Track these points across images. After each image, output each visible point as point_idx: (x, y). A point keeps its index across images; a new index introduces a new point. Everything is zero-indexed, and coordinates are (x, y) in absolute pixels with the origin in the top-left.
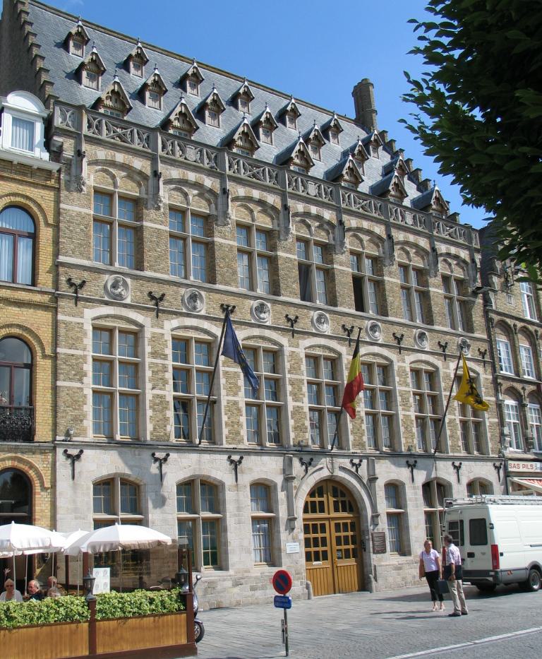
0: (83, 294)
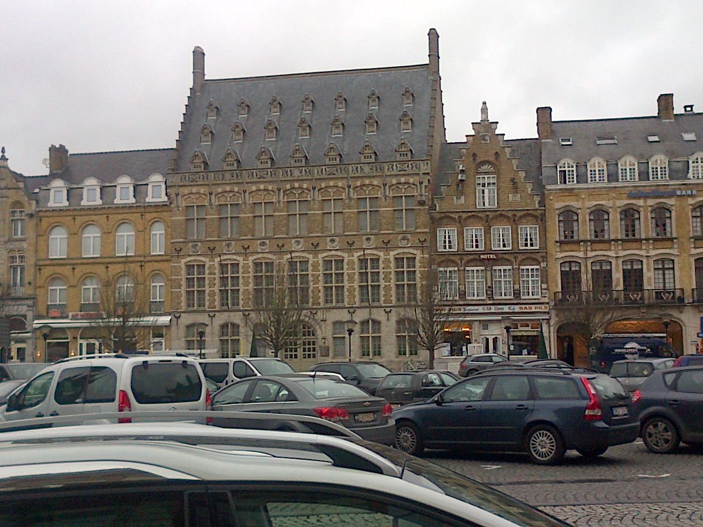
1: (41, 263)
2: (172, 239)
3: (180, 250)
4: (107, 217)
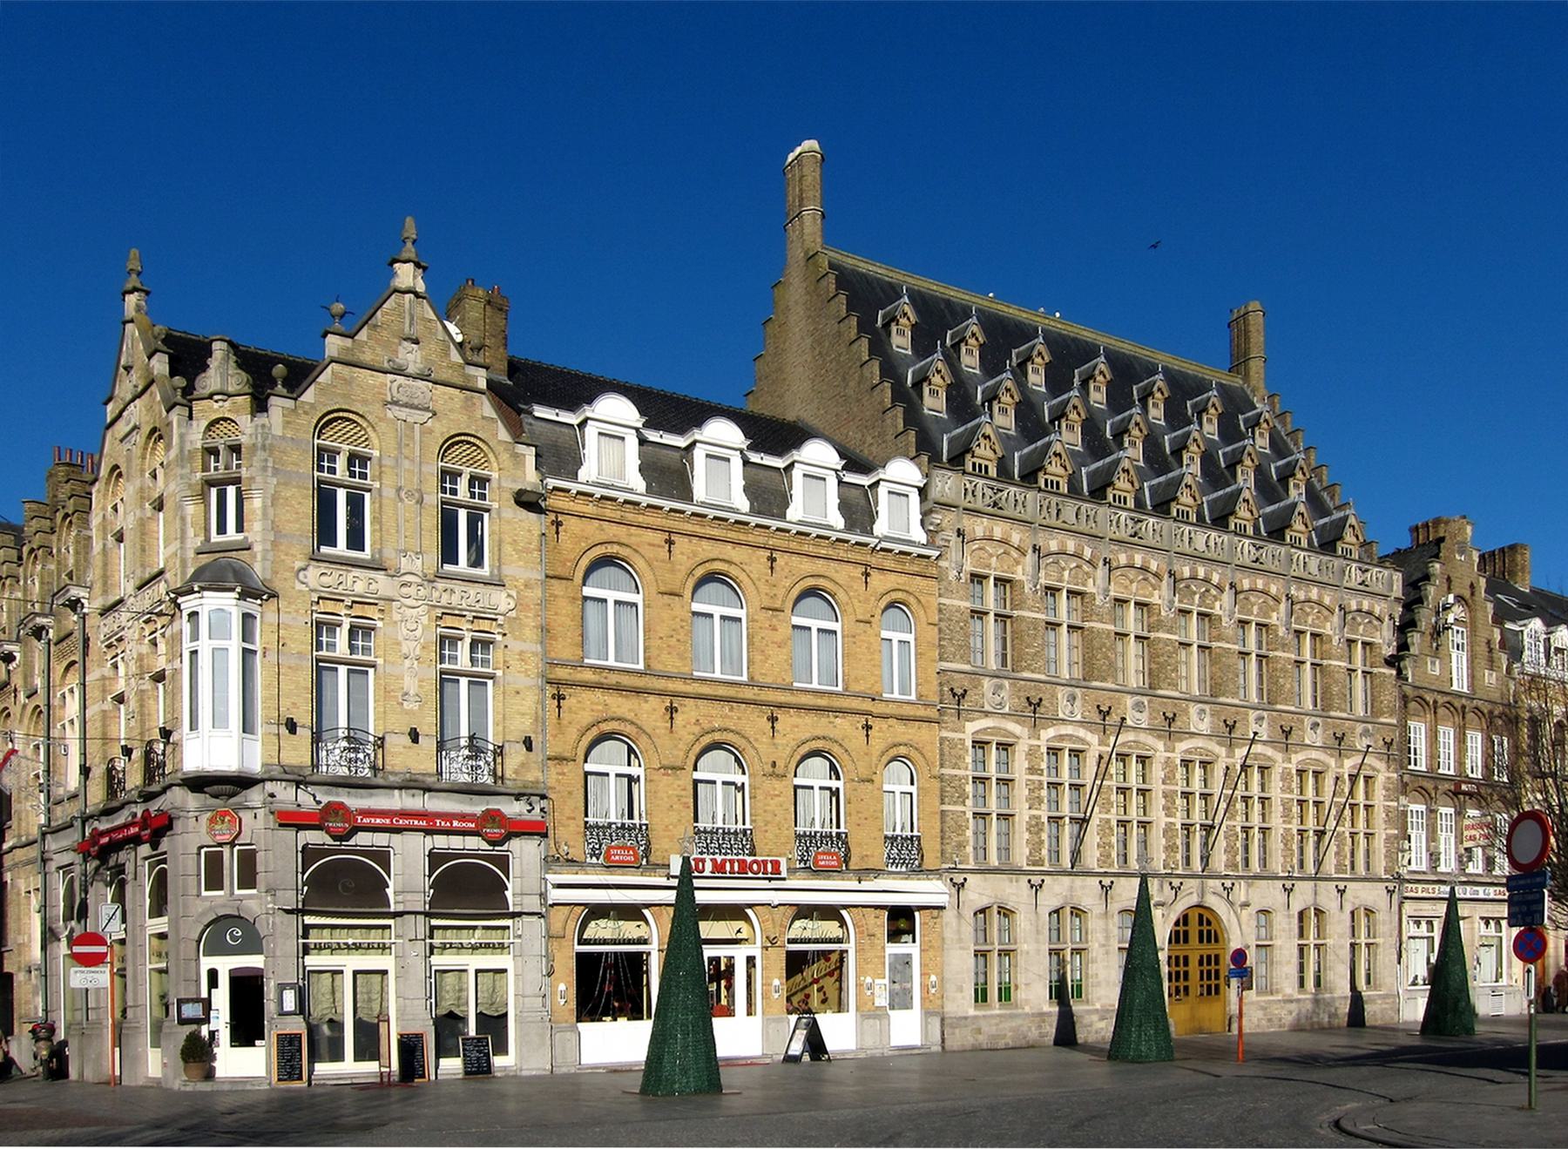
0: (965, 705)
1: (562, 673)
2: (941, 660)
3: (963, 696)
4: (772, 560)
